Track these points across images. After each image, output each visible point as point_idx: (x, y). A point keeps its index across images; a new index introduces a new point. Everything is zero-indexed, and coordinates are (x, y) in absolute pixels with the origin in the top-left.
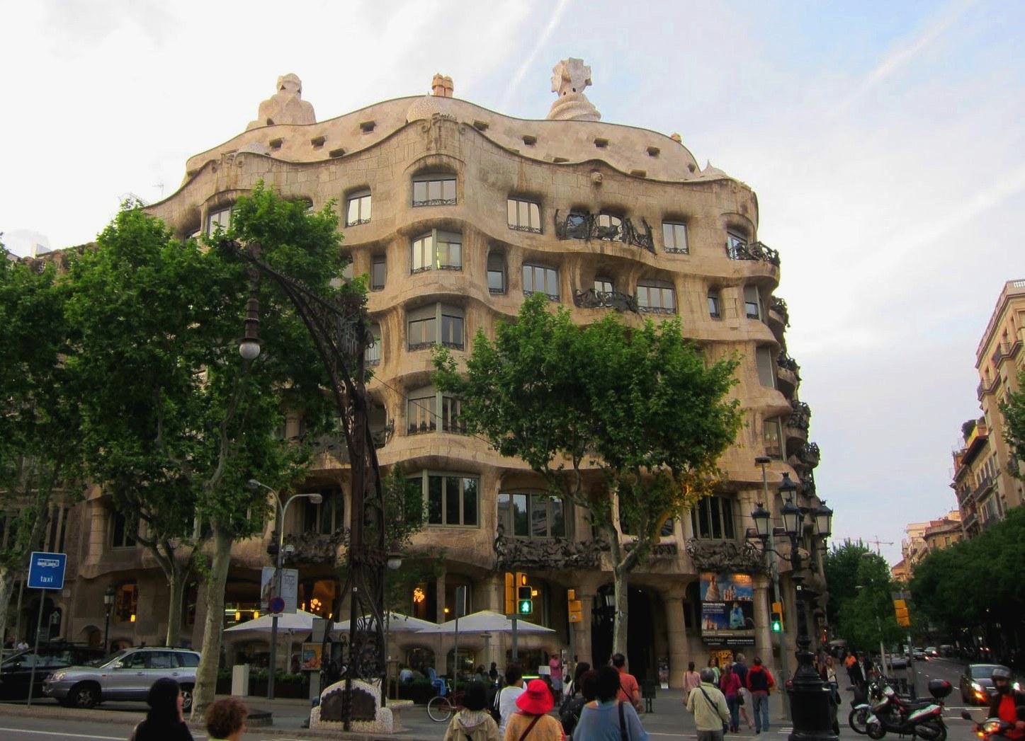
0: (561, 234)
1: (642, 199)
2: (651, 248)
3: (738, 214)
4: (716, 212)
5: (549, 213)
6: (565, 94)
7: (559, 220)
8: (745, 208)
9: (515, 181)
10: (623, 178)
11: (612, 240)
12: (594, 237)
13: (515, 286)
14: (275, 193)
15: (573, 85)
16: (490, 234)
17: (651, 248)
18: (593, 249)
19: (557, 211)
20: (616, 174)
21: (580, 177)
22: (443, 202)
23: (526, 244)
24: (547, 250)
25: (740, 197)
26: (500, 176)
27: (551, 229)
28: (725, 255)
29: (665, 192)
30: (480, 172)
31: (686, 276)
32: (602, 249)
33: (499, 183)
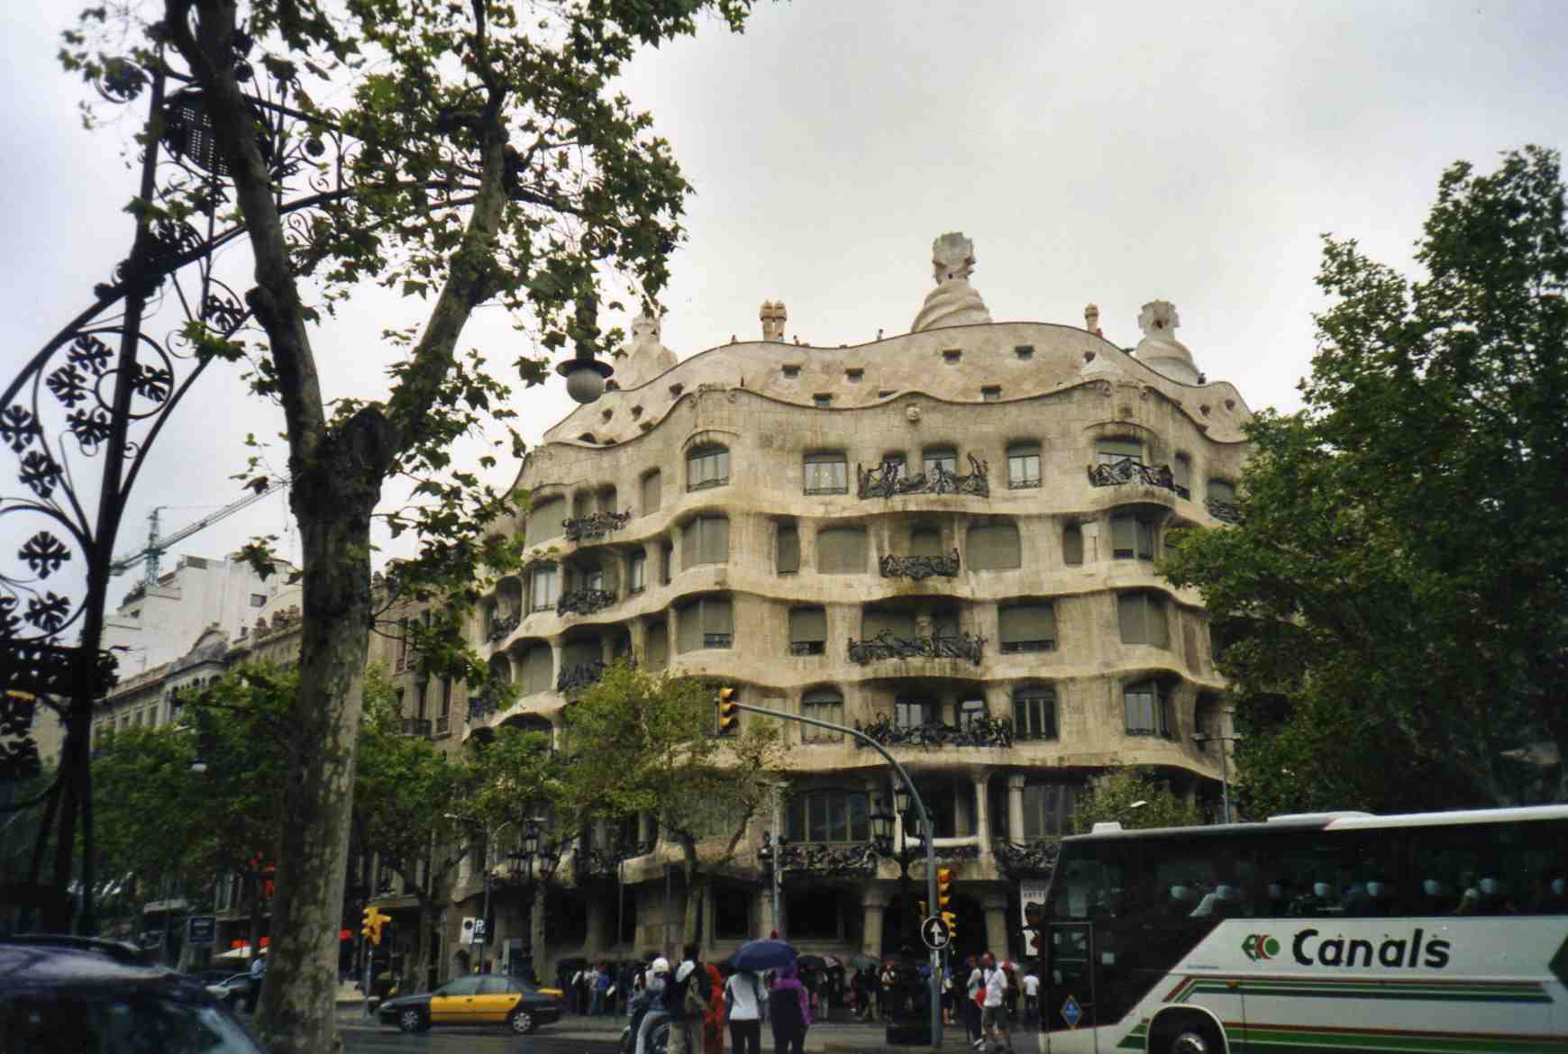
1: (972, 428)
2: (982, 491)
4: (1077, 427)
5: (853, 467)
8: (1127, 411)
13: (807, 563)
14: (583, 485)
15: (948, 271)
16: (769, 509)
17: (982, 491)
22: (716, 483)
23: (819, 512)
24: (846, 514)
27: (854, 488)
28: (1087, 481)
31: (1029, 517)
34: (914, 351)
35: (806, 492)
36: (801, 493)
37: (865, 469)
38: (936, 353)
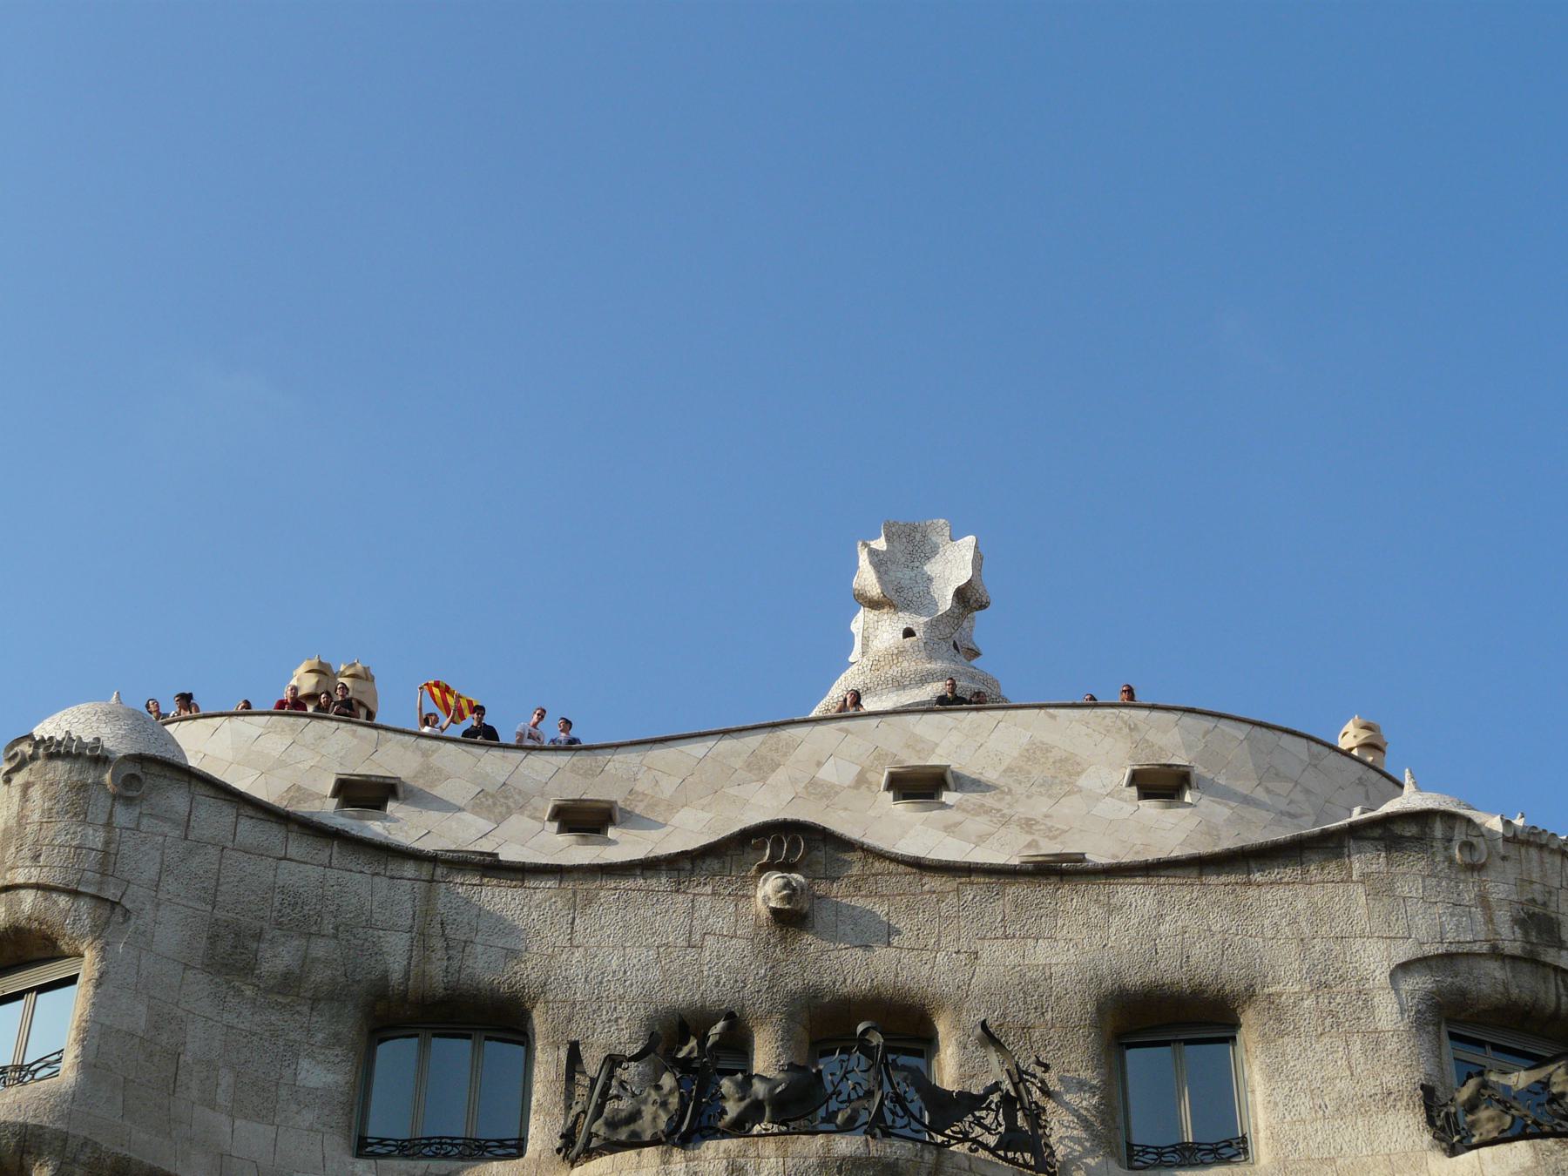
3: (1496, 953)
9: (395, 955)
10: (908, 878)
20: (878, 866)
21: (705, 905)
25: (1500, 888)
26: (320, 949)
30: (214, 939)
33: (321, 975)
35: (363, 1147)
36: (336, 1148)
37: (592, 1063)
38: (861, 780)
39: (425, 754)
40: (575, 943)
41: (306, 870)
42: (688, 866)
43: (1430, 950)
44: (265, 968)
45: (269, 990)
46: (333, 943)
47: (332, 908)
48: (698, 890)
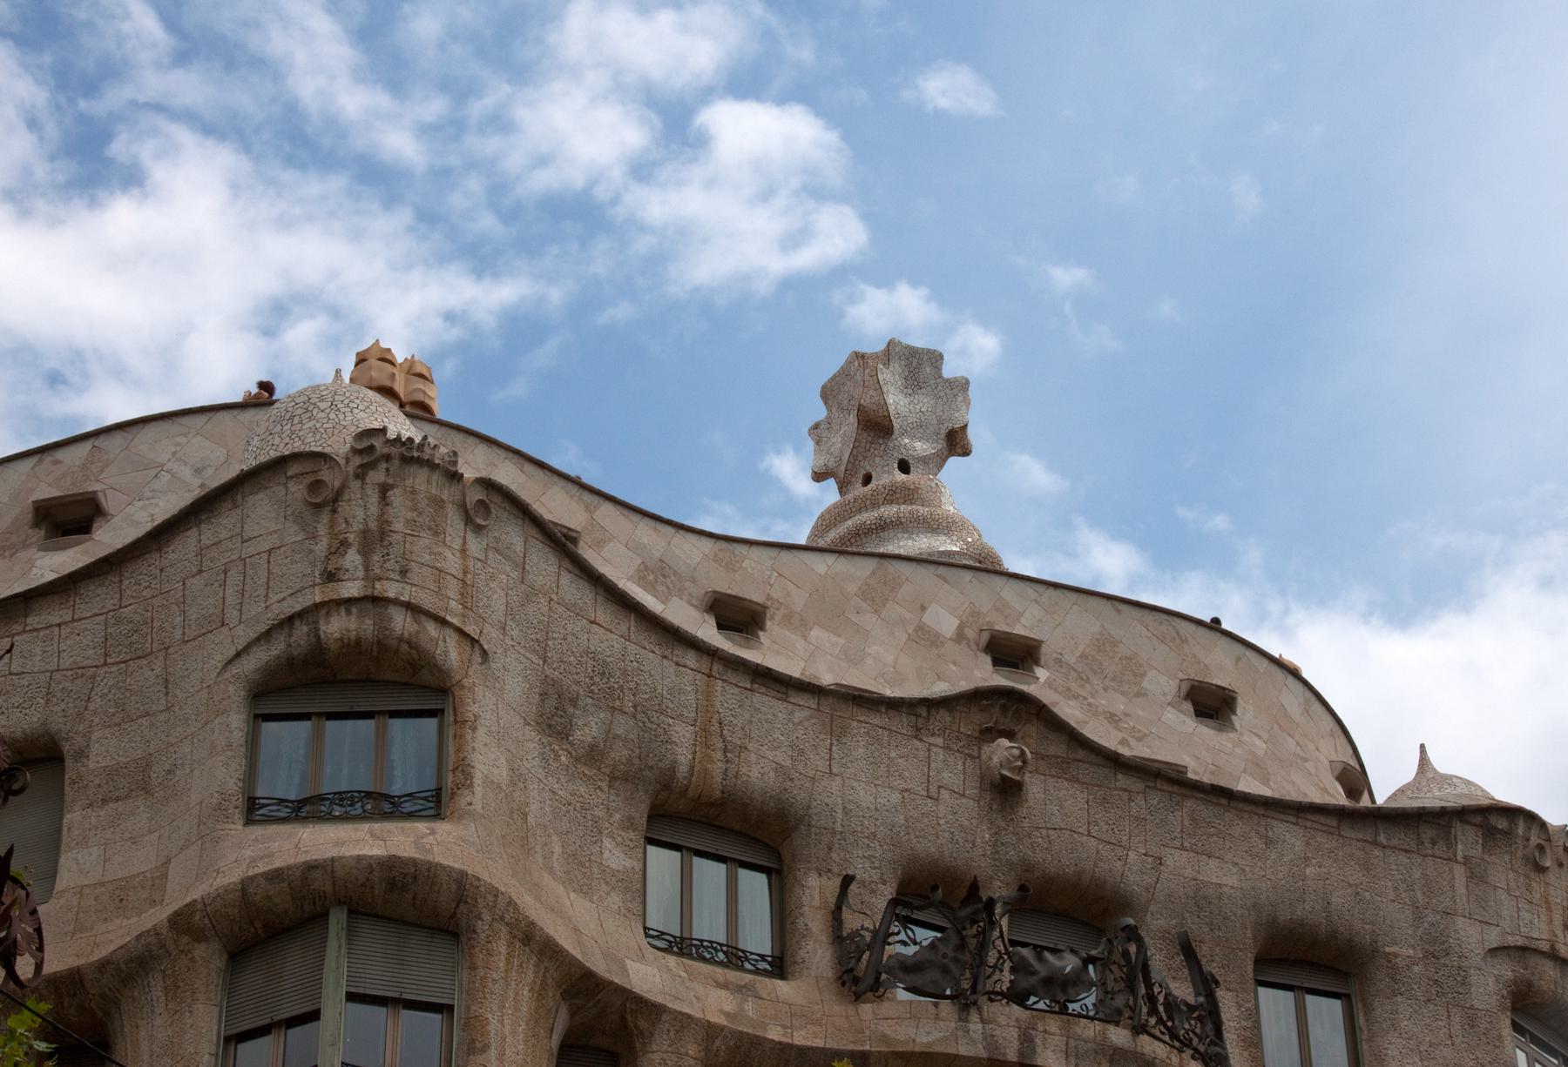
0: (859, 978)
4: (1472, 937)
6: (867, 479)
7: (852, 921)
9: (682, 747)
11: (1063, 1010)
12: (992, 996)
16: (566, 942)
18: (990, 1041)
19: (847, 880)
20: (1081, 754)
21: (939, 755)
27: (817, 955)
29: (1269, 843)
30: (544, 695)
32: (1026, 1040)
33: (619, 754)
34: (893, 610)
38: (960, 636)
39: (587, 509)
40: (835, 770)
41: (610, 638)
42: (924, 714)
43: (1511, 940)
44: (578, 735)
45: (578, 760)
46: (631, 722)
47: (632, 685)
48: (931, 740)
